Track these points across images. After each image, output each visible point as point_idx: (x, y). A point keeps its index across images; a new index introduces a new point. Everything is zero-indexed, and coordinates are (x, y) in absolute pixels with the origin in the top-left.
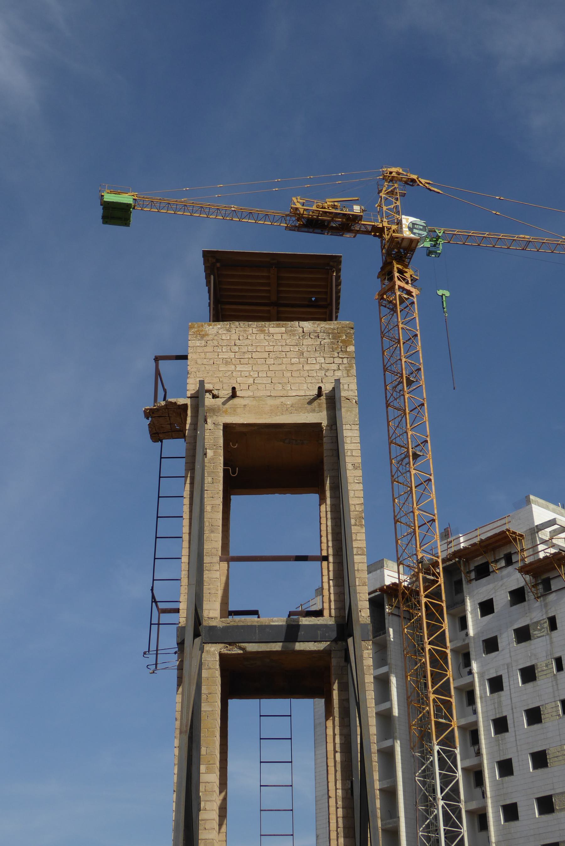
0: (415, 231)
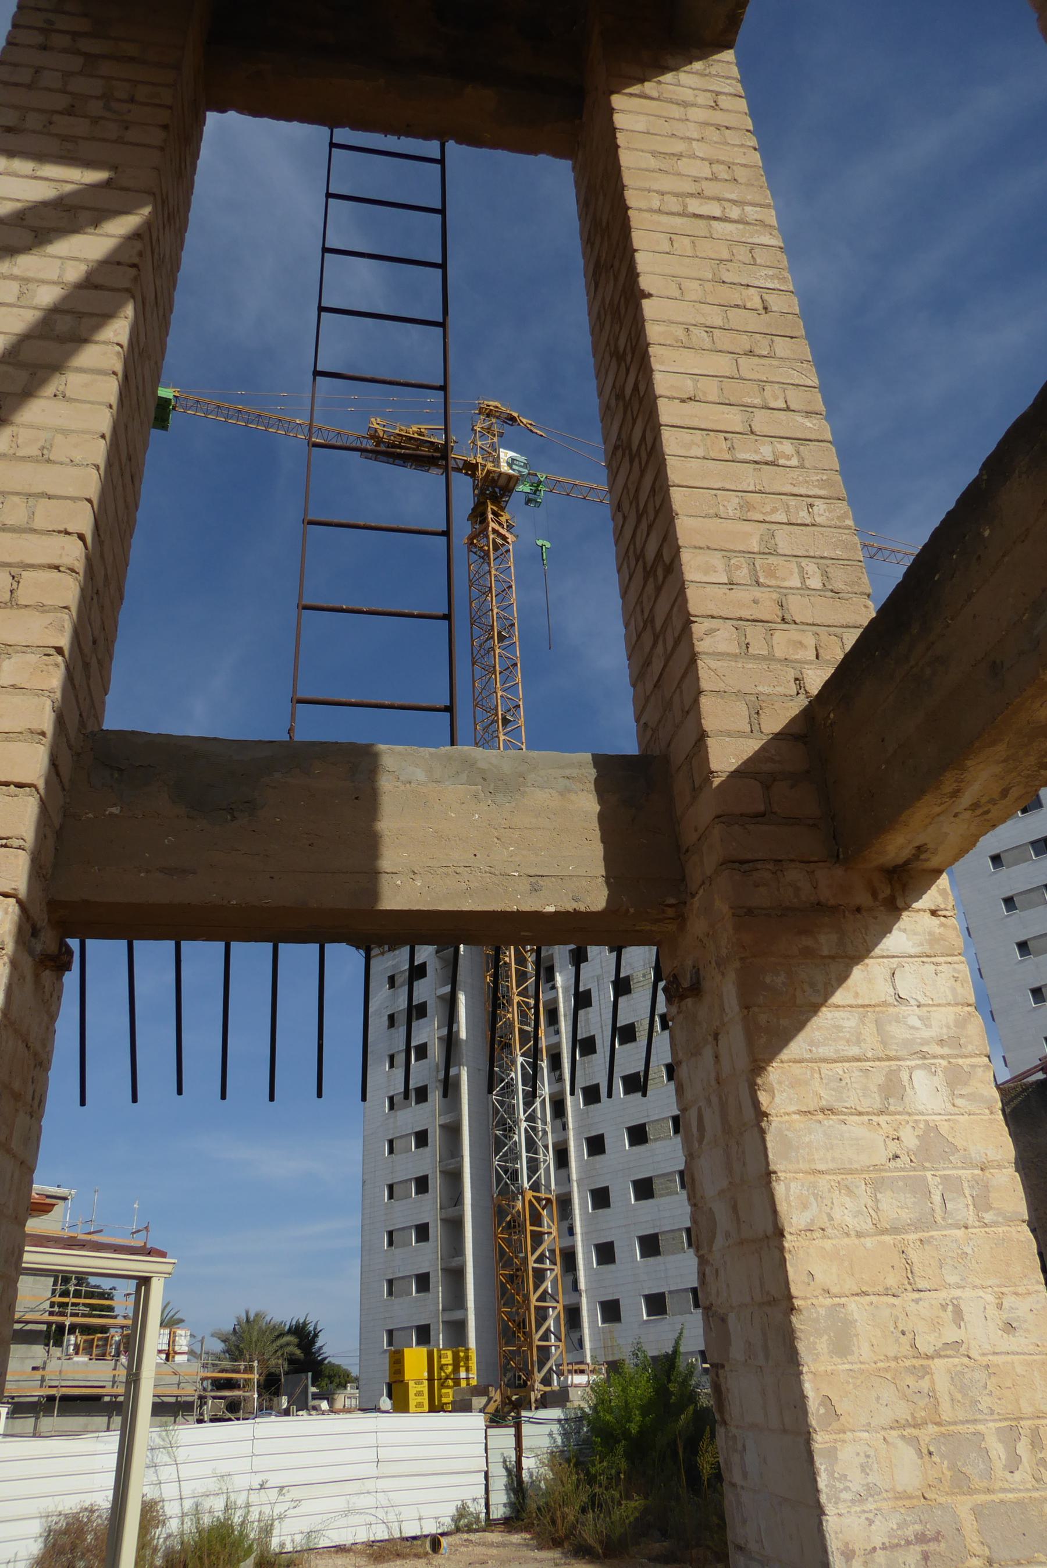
0: (514, 467)
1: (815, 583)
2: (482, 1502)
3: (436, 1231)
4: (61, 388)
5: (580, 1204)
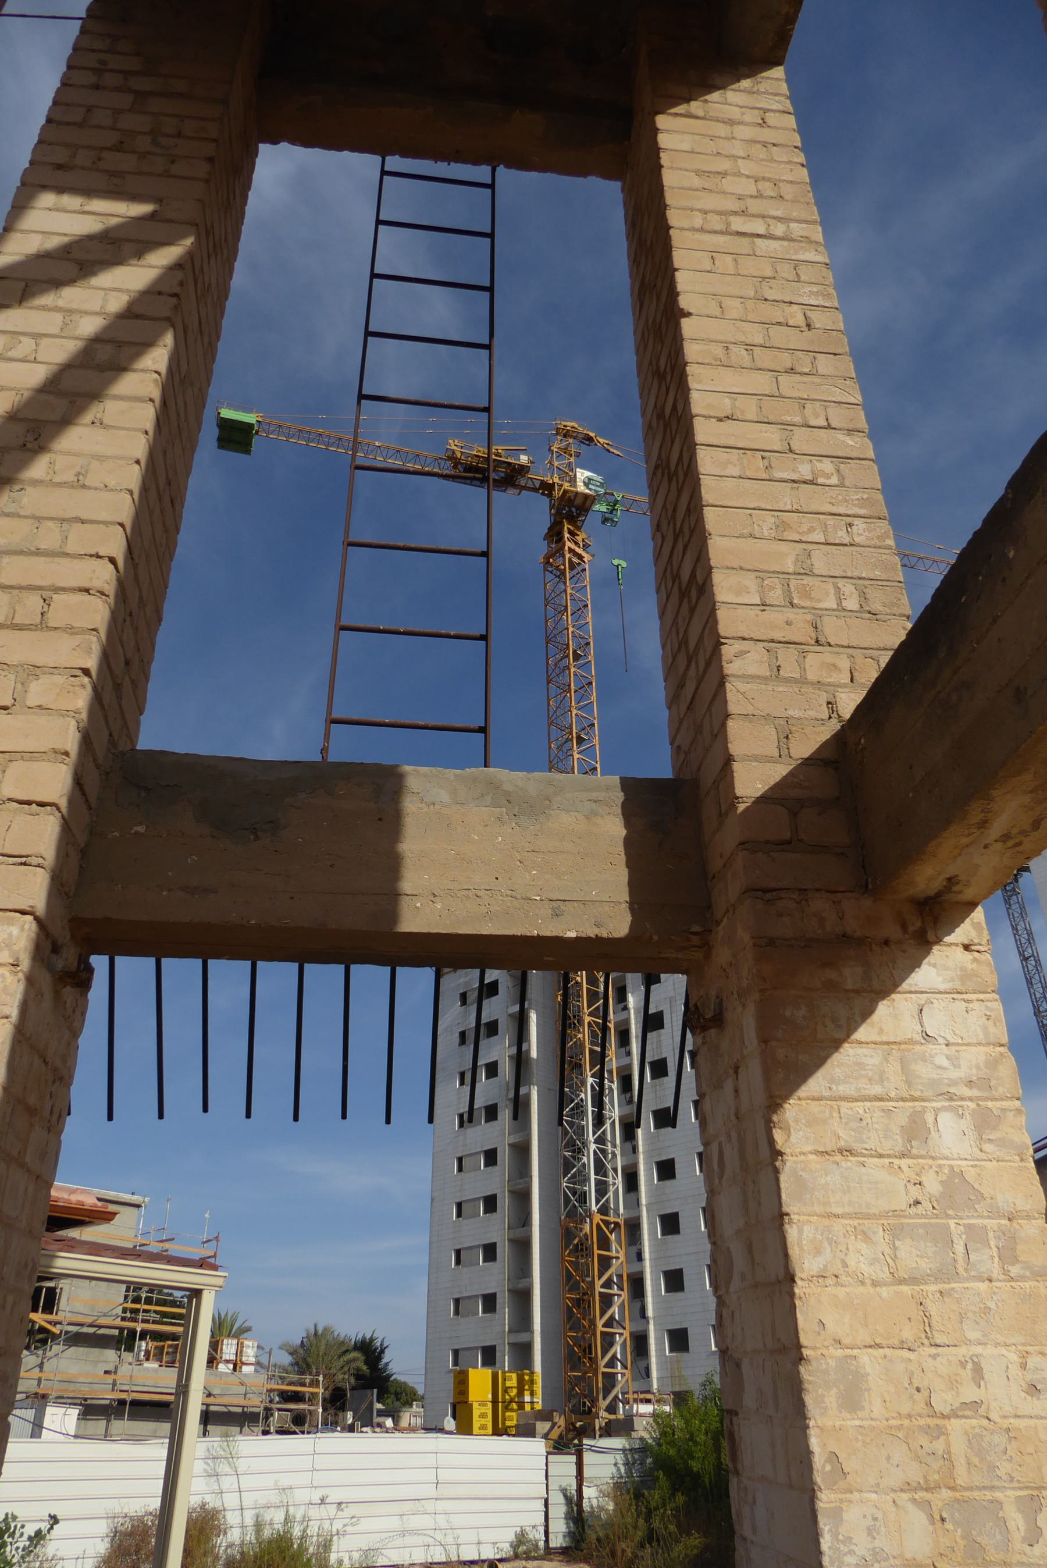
0: (591, 486)
1: (852, 604)
2: (542, 1529)
3: (504, 1251)
4: (99, 416)
5: (649, 1229)
